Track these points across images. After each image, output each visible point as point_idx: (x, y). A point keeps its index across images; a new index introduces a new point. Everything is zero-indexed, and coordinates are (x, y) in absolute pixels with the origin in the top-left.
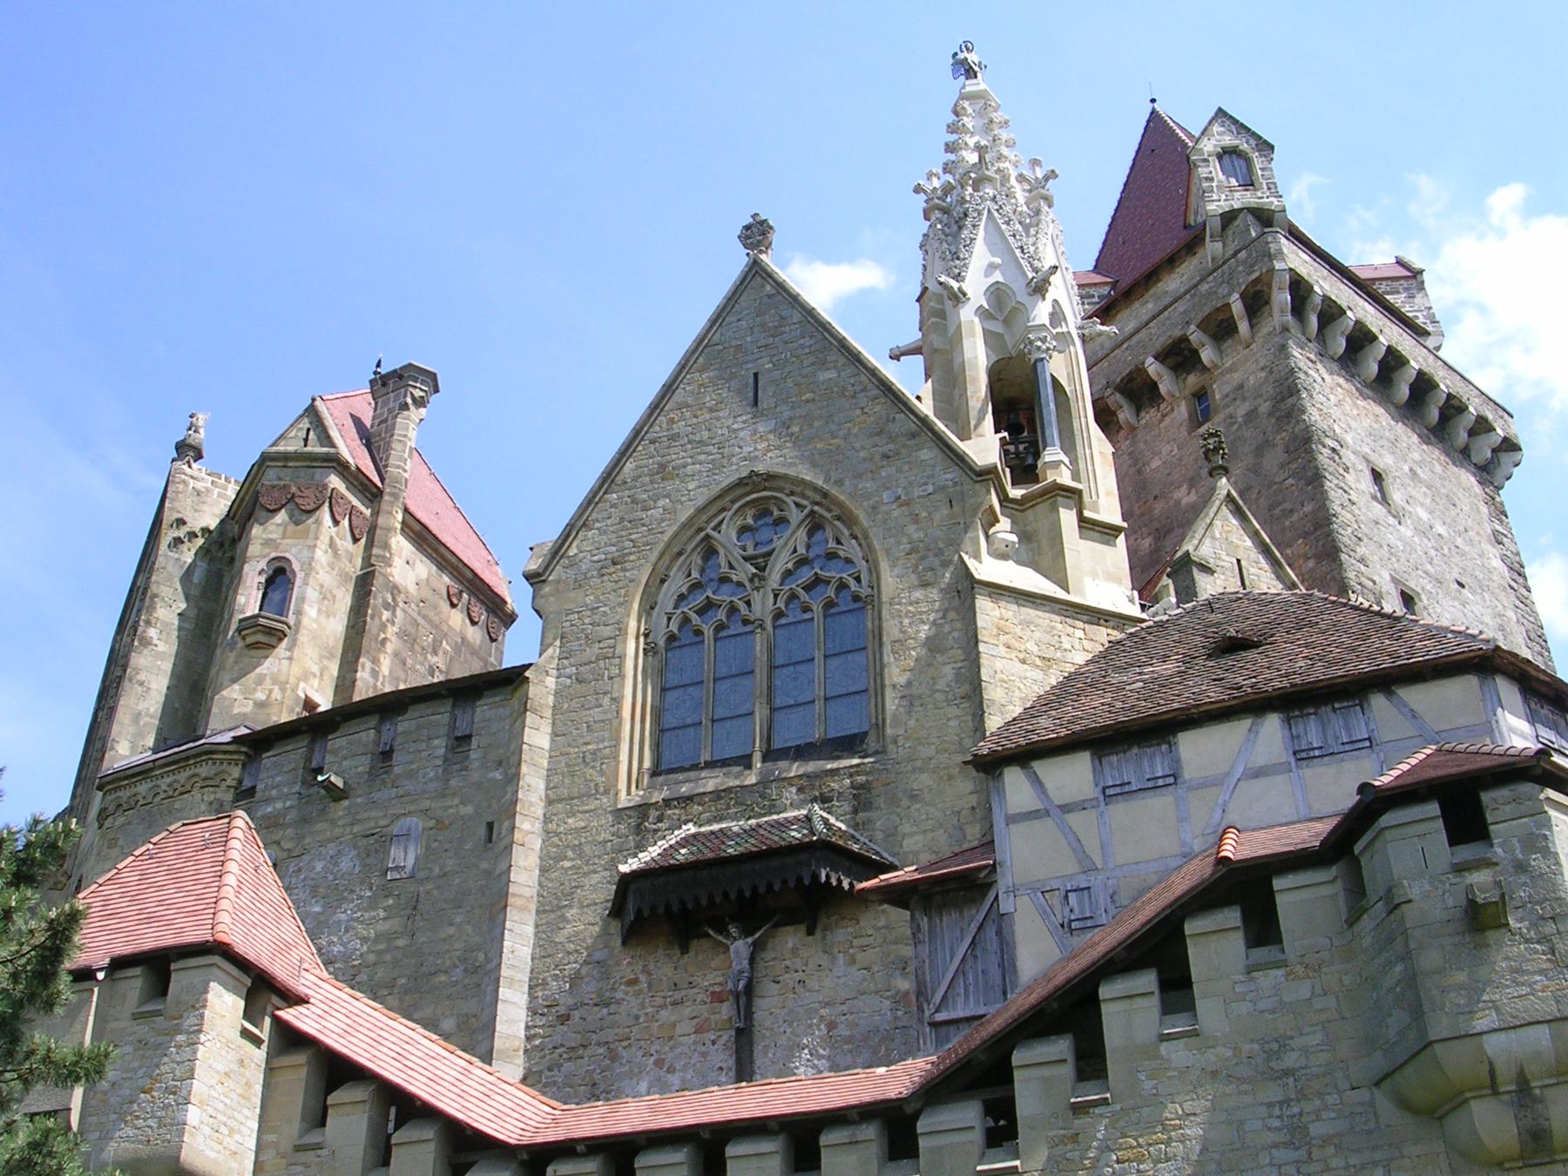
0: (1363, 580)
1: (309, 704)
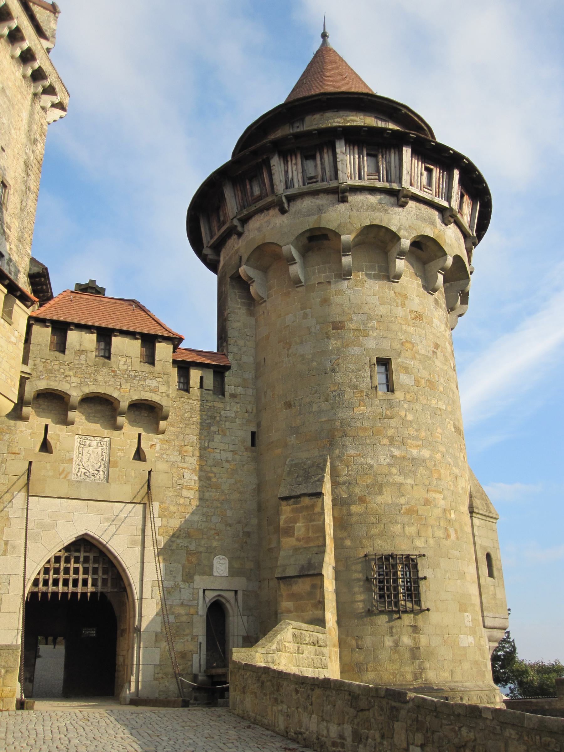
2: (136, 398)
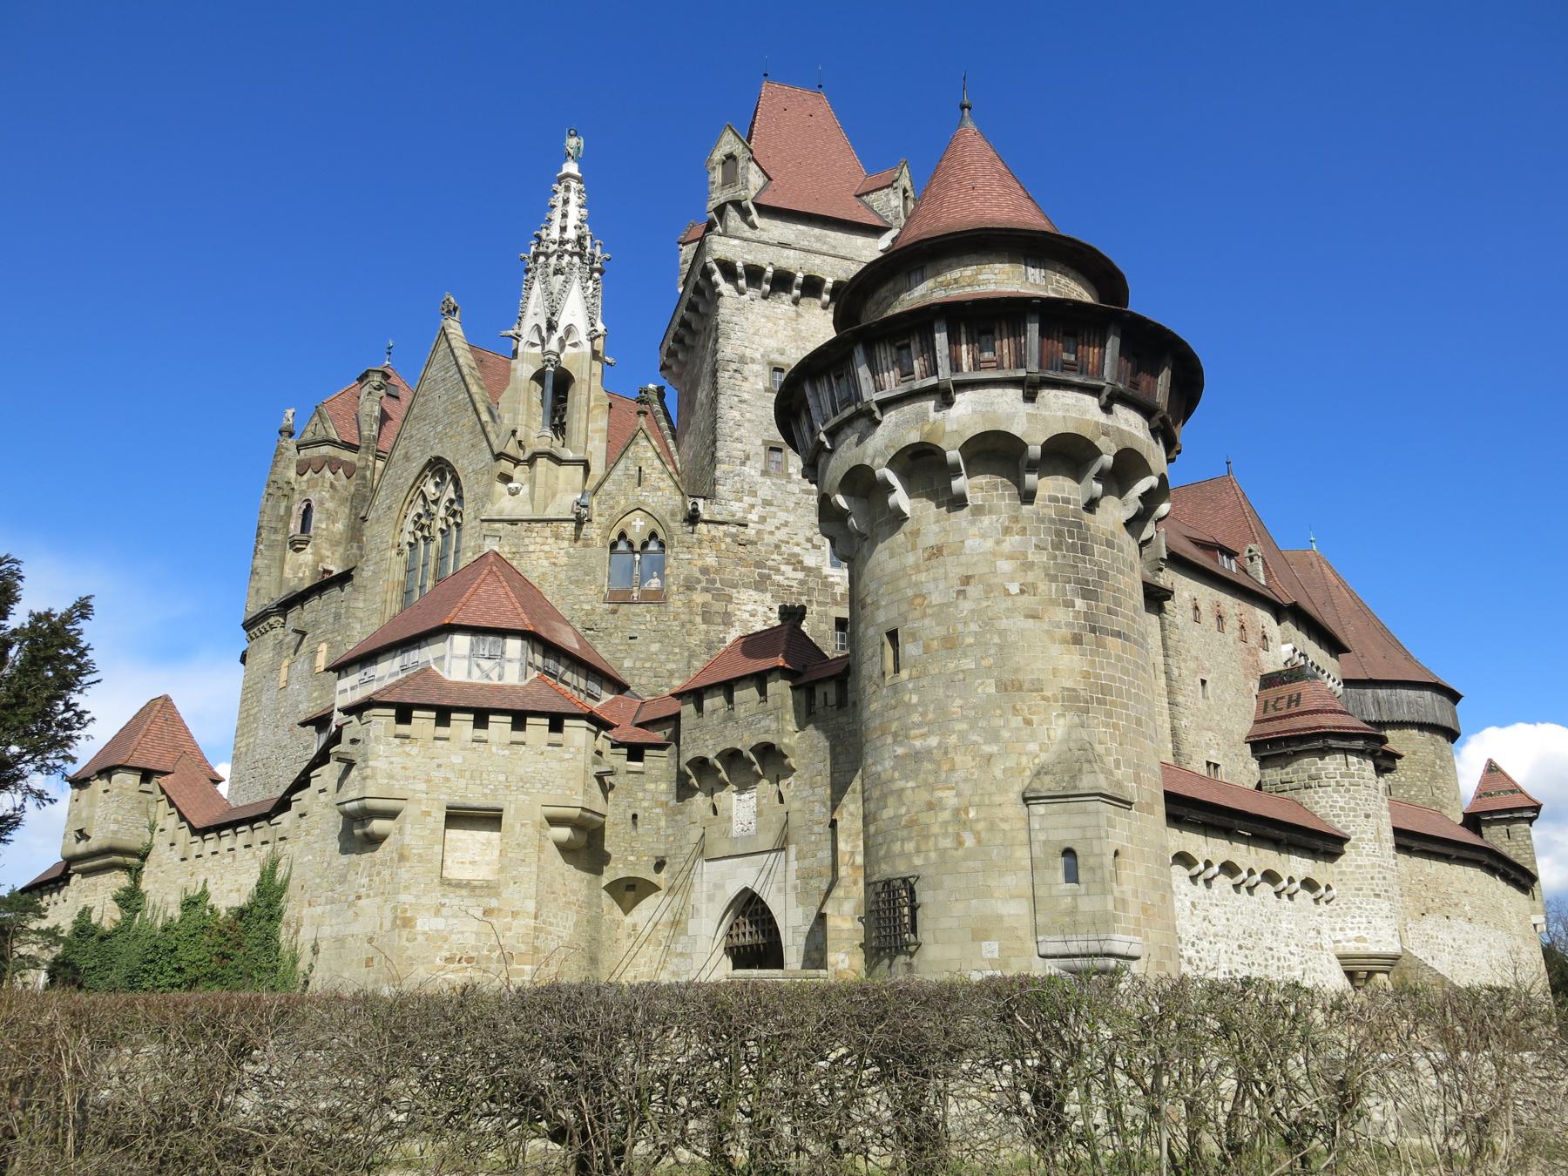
0: (735, 453)
1: (326, 571)
2: (754, 743)
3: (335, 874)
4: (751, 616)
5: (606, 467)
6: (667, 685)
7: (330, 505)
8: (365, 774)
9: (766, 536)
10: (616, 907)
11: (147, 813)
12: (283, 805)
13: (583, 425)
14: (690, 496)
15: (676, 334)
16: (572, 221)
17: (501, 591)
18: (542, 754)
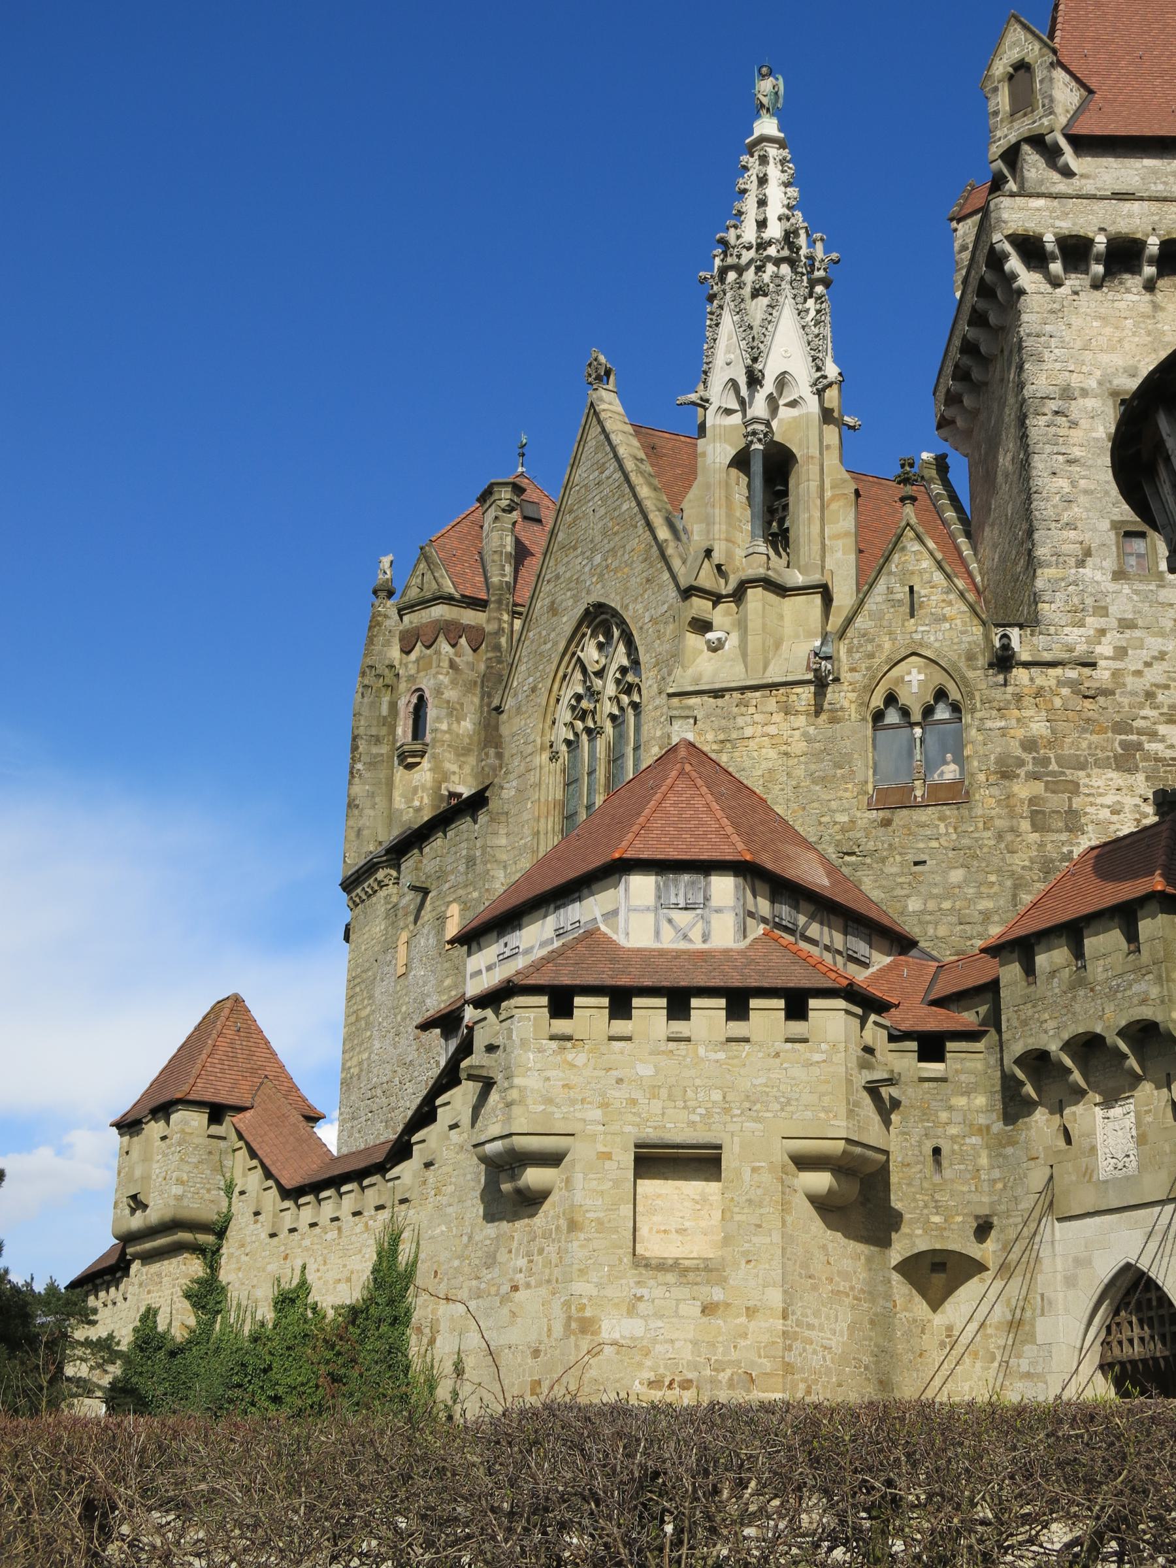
0: (1067, 548)
1: (452, 795)
2: (1123, 1023)
3: (480, 1254)
4: (1112, 813)
5: (858, 591)
6: (980, 936)
7: (451, 694)
8: (509, 1099)
9: (1129, 680)
10: (918, 1298)
11: (220, 1168)
12: (401, 1150)
13: (815, 529)
14: (997, 625)
15: (956, 366)
16: (775, 209)
17: (699, 803)
18: (777, 1055)
